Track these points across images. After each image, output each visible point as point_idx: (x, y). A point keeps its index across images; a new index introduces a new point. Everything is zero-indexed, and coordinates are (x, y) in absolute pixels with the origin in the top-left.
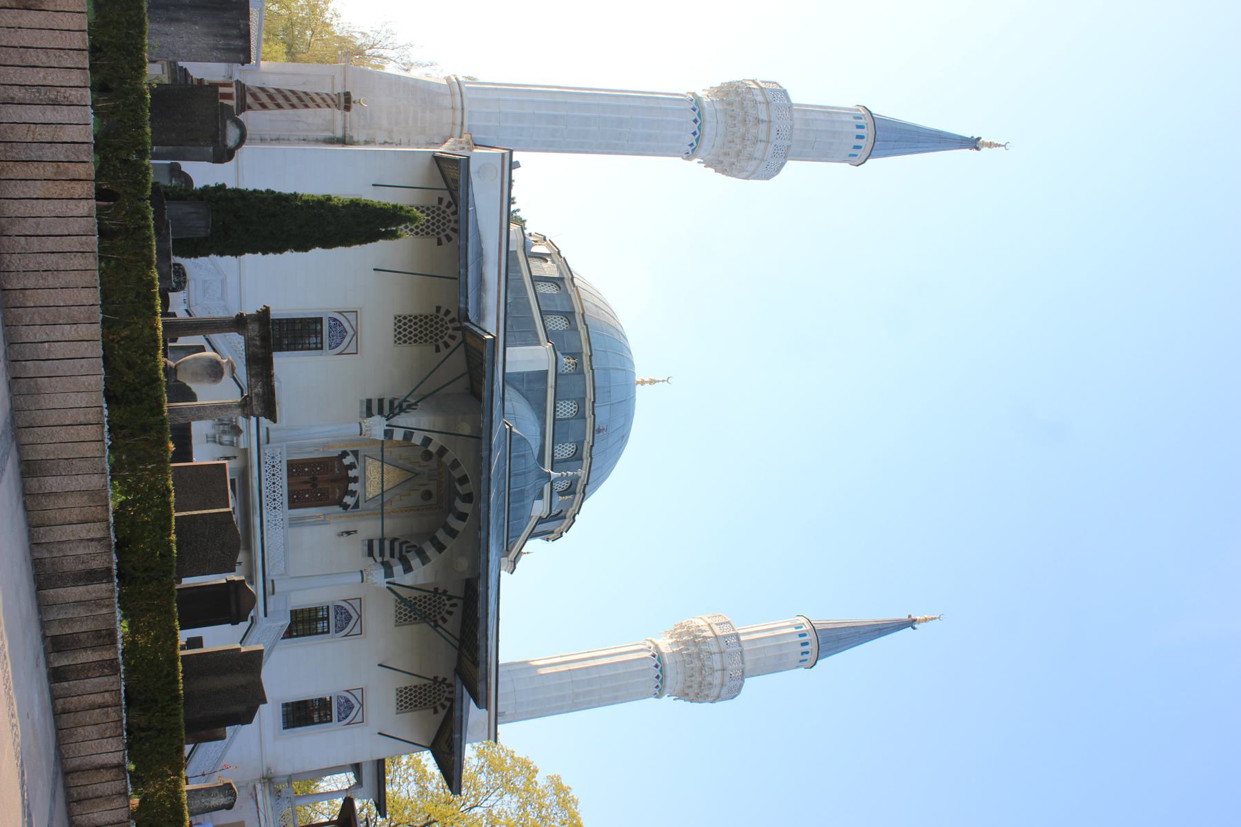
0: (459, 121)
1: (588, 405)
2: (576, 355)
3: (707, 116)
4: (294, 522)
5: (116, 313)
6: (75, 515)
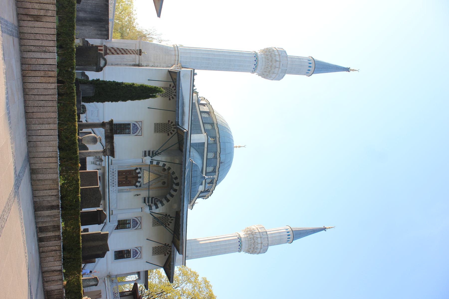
0: (177, 59)
2: (215, 137)
3: (259, 59)
4: (120, 191)
5: (63, 121)
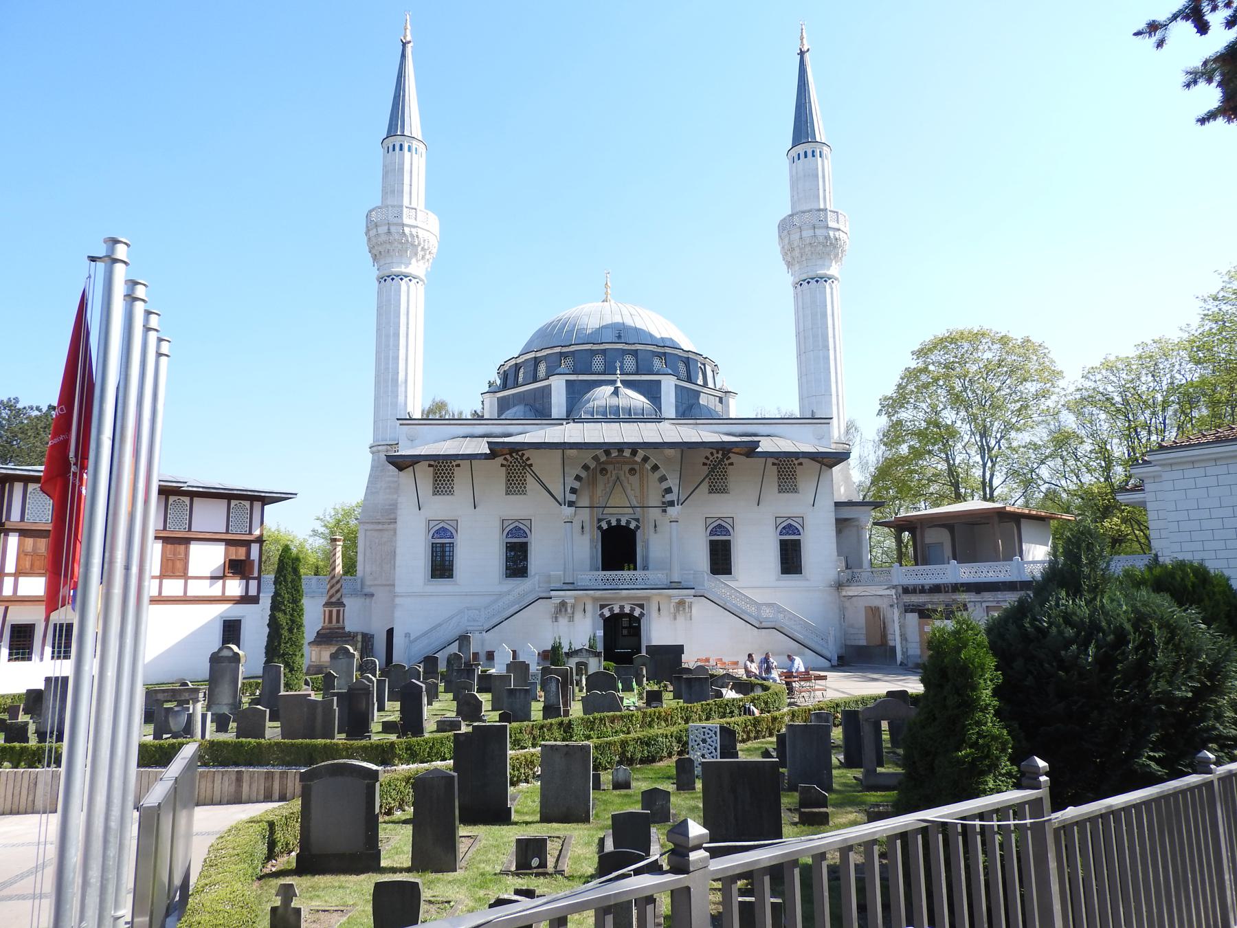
1: (596, 347)
2: (563, 355)
6: (209, 785)
